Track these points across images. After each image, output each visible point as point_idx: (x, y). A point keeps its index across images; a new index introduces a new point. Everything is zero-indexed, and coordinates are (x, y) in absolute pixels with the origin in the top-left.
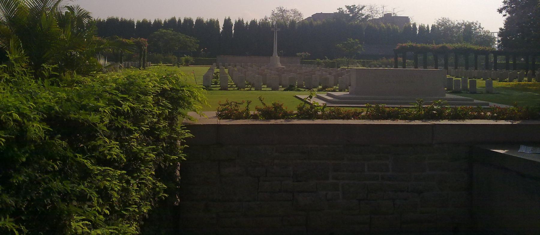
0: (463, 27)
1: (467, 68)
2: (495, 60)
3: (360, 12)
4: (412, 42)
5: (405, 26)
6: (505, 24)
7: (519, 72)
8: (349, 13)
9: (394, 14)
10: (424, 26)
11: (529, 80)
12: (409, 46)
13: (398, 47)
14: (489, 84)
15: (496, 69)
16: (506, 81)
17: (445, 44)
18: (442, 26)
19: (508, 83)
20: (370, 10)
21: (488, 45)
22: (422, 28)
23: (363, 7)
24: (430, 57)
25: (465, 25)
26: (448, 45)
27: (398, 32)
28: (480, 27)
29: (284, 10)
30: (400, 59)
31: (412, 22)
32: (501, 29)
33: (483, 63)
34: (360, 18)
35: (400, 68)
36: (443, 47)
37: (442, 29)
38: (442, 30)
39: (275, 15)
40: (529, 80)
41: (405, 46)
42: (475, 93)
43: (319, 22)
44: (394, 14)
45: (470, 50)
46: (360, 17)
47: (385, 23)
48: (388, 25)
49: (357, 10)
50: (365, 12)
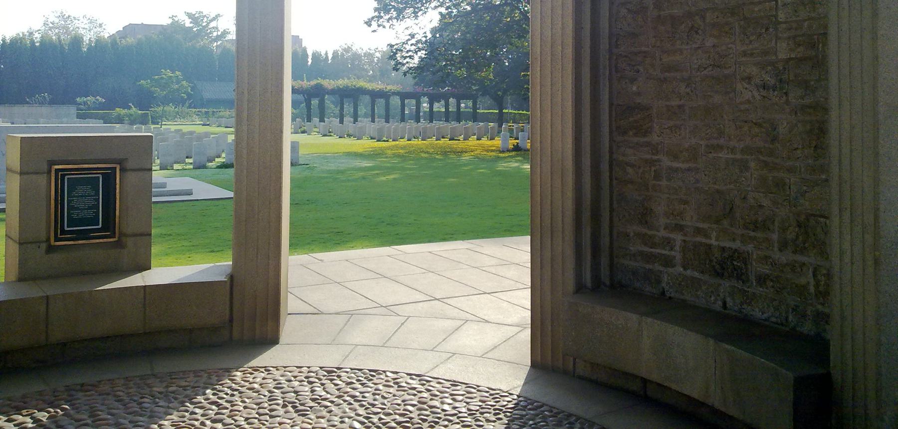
2: (431, 107)
3: (213, 24)
8: (192, 25)
17: (320, 81)
23: (218, 16)
33: (383, 112)
34: (211, 35)
43: (130, 40)
45: (362, 91)
46: (211, 33)
49: (205, 19)
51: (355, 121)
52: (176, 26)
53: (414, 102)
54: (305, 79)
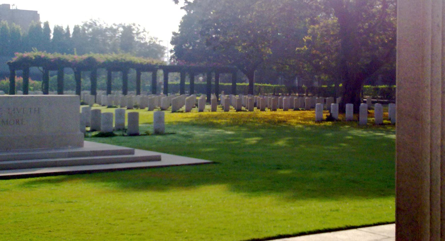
0: (121, 29)
1: (125, 93)
2: (166, 79)
4: (39, 50)
5: (32, 26)
6: (180, 26)
7: (199, 96)
9: (14, 5)
11: (214, 110)
12: (35, 56)
13: (14, 59)
14: (159, 119)
15: (166, 92)
16: (182, 112)
17: (92, 55)
18: (90, 26)
19: (185, 115)
21: (156, 57)
22: (58, 30)
24: (69, 76)
25: (124, 27)
28: (144, 31)
30: (19, 80)
31: (43, 20)
32: (174, 33)
35: (19, 94)
36: (90, 61)
37: (89, 32)
38: (90, 34)
40: (214, 110)
41: (27, 57)
42: (136, 134)
44: (14, 5)
48: (3, 23)
51: (109, 92)
53: (149, 74)
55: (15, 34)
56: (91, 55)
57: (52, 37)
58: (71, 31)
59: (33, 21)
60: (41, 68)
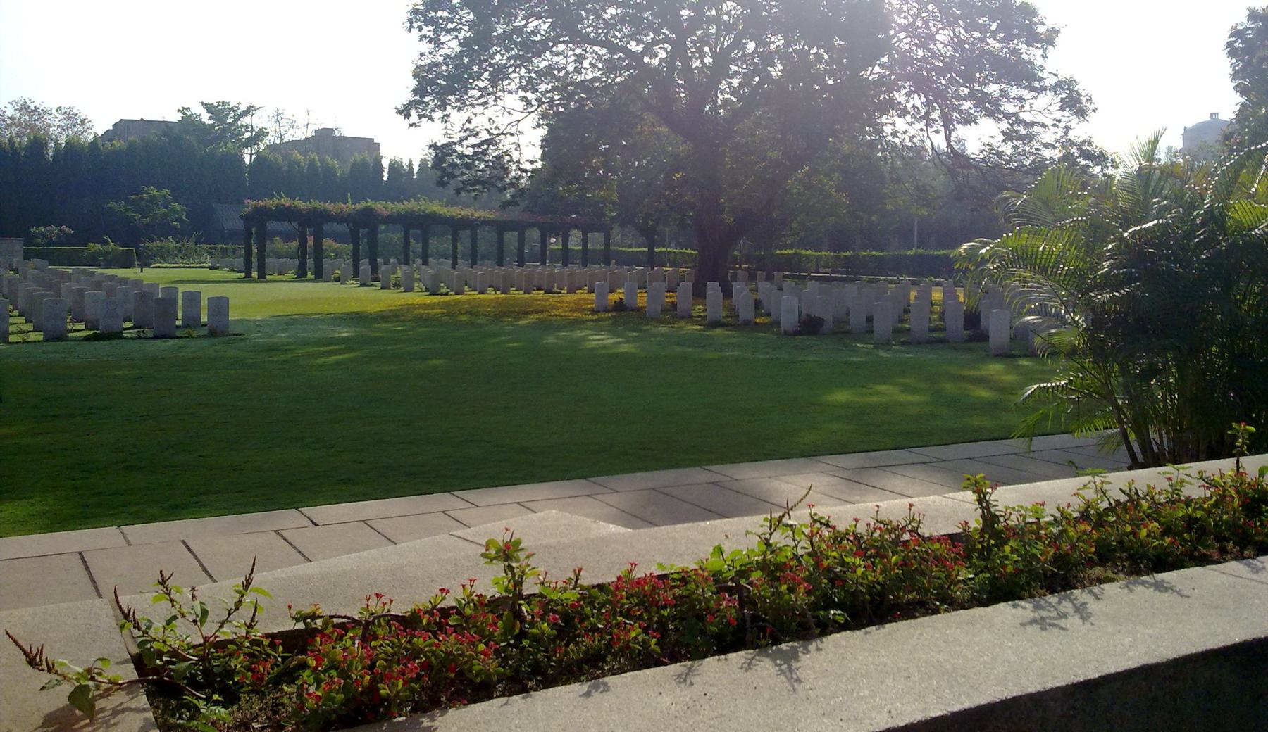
3: (246, 120)
5: (355, 161)
8: (212, 122)
10: (402, 162)
17: (370, 203)
20: (275, 119)
26: (379, 206)
27: (335, 174)
29: (36, 109)
36: (368, 212)
39: (9, 122)
47: (304, 154)
49: (232, 114)
50: (258, 121)
52: (188, 122)
54: (349, 200)
55: (330, 171)
56: (369, 204)
57: (385, 178)
58: (416, 168)
59: (356, 154)
60: (295, 224)
